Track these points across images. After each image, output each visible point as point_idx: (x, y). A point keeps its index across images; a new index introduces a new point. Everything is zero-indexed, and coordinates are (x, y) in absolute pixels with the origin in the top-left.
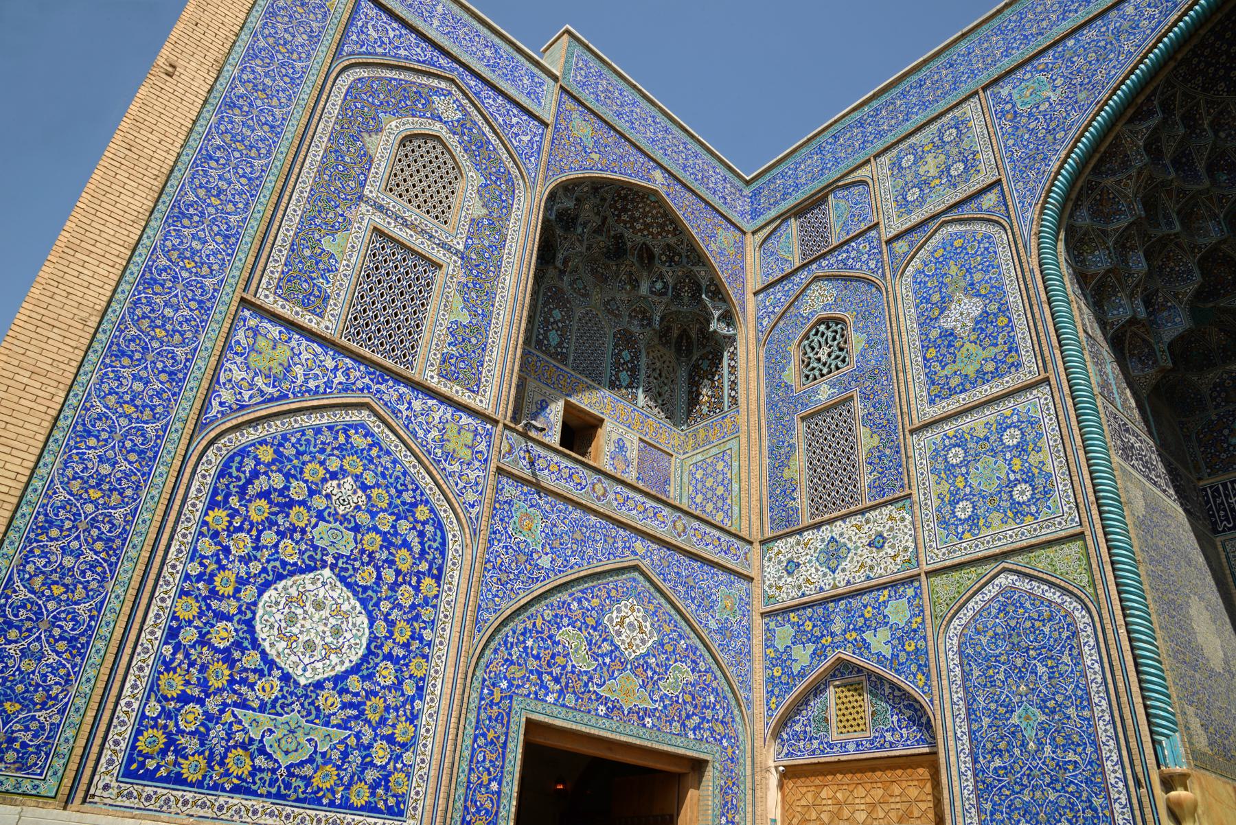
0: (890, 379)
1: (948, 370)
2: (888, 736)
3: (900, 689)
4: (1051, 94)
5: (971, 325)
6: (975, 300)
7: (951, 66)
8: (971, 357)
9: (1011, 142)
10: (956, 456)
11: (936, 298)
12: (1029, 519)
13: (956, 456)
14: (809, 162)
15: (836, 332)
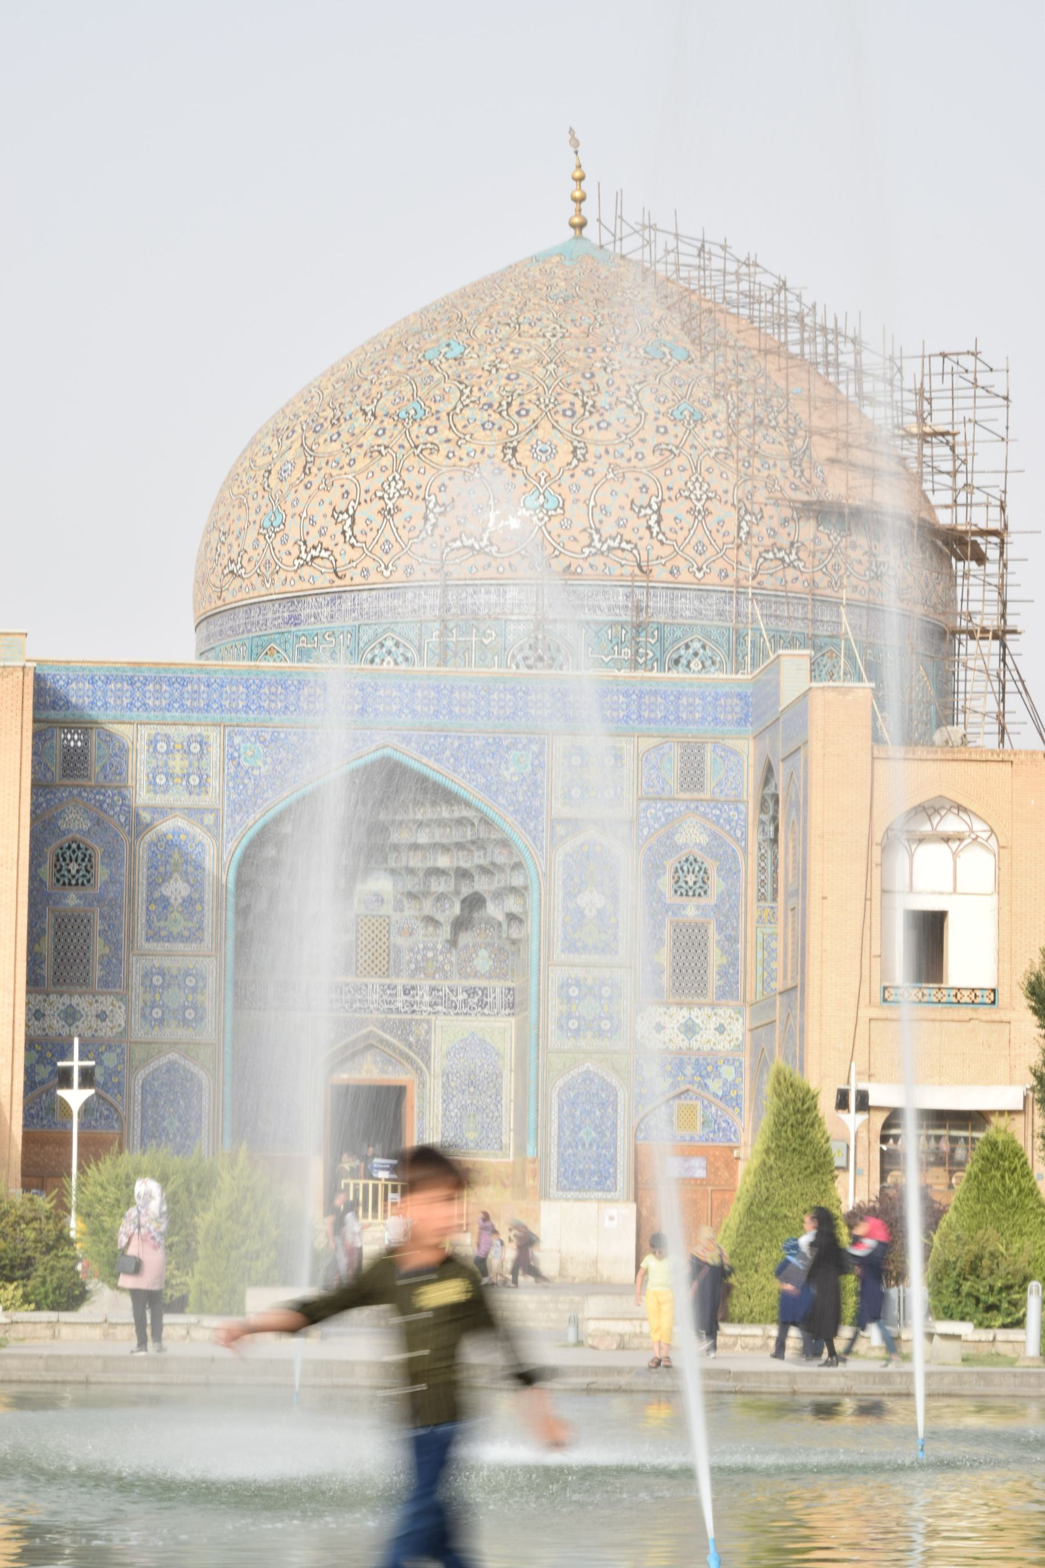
0: (121, 911)
1: (162, 924)
2: (93, 1123)
3: (103, 1098)
4: (261, 765)
5: (180, 900)
6: (186, 884)
7: (208, 686)
8: (178, 923)
9: (231, 784)
10: (157, 980)
11: (162, 869)
12: (191, 1029)
13: (157, 980)
14: (81, 685)
15: (85, 855)
